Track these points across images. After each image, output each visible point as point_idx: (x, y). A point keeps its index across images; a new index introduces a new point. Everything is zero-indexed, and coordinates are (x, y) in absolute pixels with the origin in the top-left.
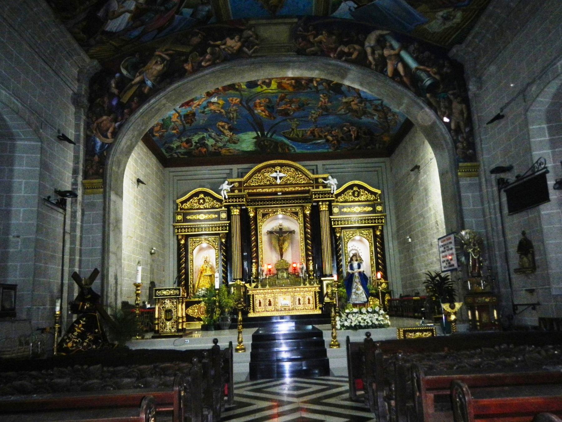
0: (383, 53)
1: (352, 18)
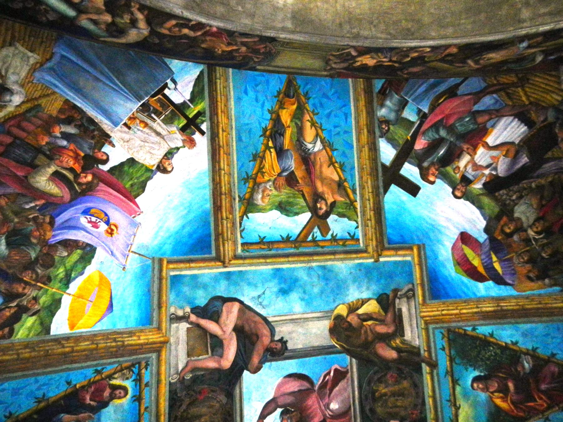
0: (113, 17)
1: (168, 61)
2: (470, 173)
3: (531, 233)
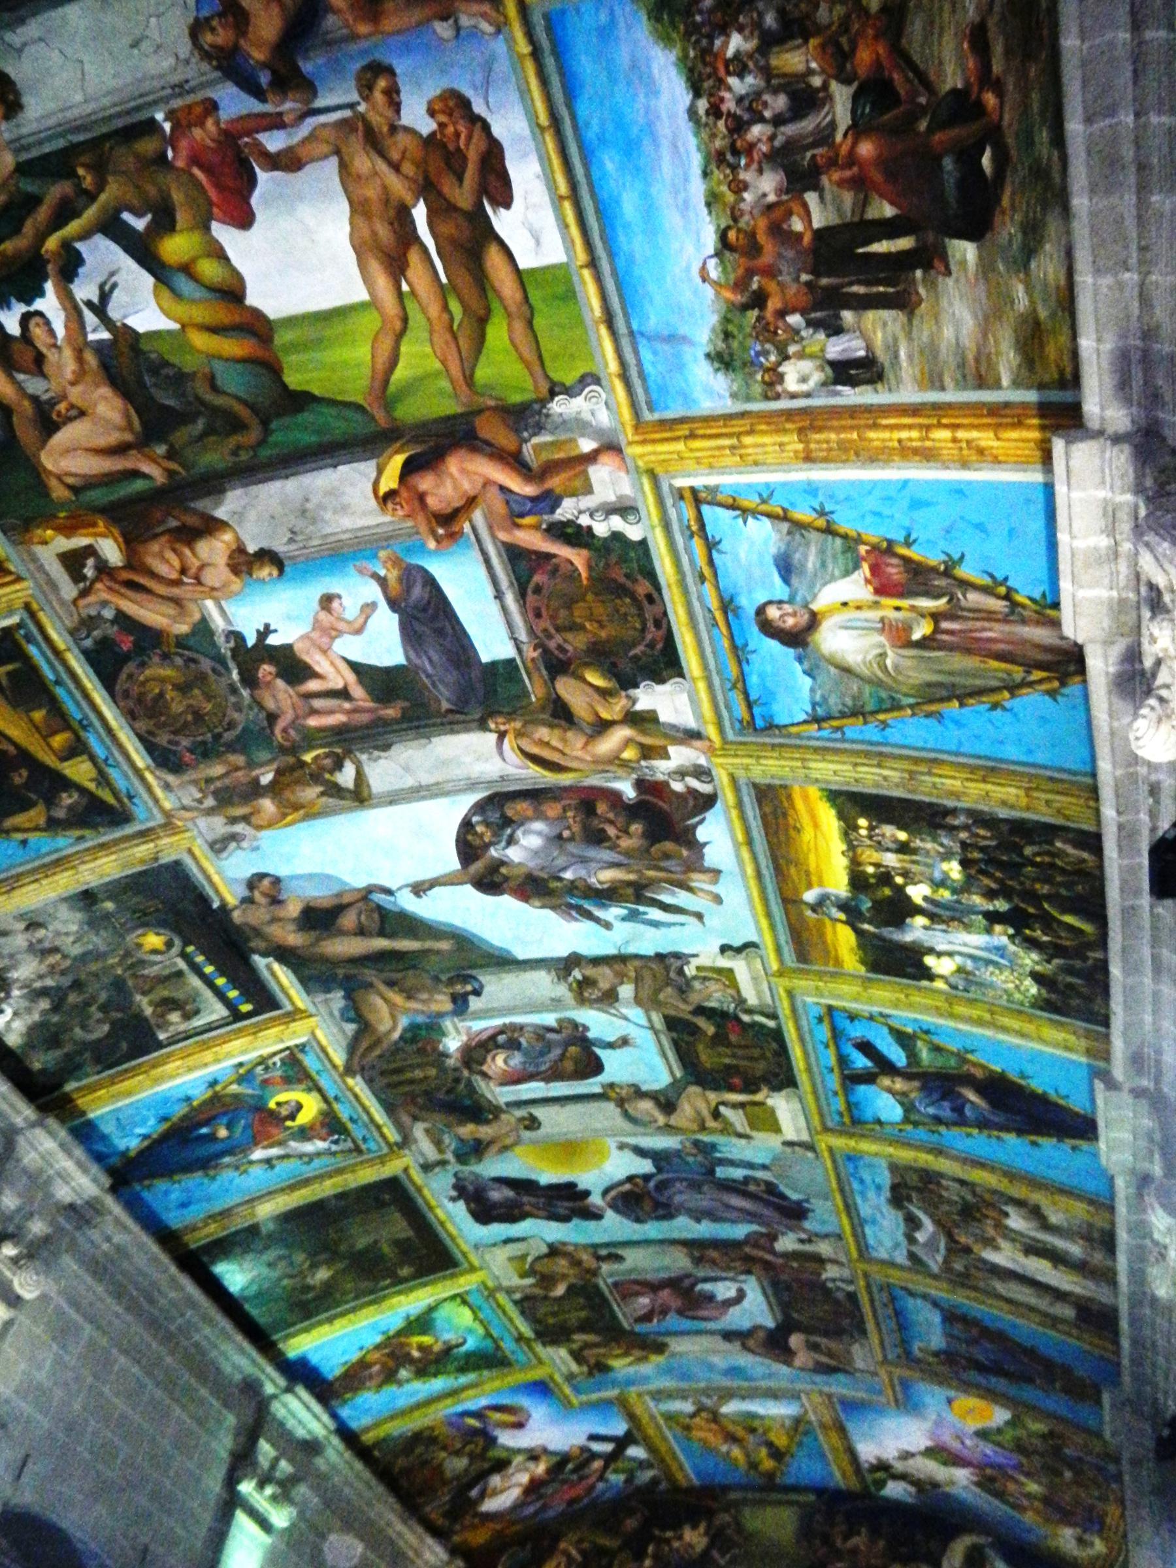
2: (531, 1465)
3: (443, 1454)
